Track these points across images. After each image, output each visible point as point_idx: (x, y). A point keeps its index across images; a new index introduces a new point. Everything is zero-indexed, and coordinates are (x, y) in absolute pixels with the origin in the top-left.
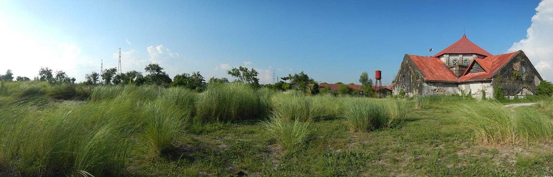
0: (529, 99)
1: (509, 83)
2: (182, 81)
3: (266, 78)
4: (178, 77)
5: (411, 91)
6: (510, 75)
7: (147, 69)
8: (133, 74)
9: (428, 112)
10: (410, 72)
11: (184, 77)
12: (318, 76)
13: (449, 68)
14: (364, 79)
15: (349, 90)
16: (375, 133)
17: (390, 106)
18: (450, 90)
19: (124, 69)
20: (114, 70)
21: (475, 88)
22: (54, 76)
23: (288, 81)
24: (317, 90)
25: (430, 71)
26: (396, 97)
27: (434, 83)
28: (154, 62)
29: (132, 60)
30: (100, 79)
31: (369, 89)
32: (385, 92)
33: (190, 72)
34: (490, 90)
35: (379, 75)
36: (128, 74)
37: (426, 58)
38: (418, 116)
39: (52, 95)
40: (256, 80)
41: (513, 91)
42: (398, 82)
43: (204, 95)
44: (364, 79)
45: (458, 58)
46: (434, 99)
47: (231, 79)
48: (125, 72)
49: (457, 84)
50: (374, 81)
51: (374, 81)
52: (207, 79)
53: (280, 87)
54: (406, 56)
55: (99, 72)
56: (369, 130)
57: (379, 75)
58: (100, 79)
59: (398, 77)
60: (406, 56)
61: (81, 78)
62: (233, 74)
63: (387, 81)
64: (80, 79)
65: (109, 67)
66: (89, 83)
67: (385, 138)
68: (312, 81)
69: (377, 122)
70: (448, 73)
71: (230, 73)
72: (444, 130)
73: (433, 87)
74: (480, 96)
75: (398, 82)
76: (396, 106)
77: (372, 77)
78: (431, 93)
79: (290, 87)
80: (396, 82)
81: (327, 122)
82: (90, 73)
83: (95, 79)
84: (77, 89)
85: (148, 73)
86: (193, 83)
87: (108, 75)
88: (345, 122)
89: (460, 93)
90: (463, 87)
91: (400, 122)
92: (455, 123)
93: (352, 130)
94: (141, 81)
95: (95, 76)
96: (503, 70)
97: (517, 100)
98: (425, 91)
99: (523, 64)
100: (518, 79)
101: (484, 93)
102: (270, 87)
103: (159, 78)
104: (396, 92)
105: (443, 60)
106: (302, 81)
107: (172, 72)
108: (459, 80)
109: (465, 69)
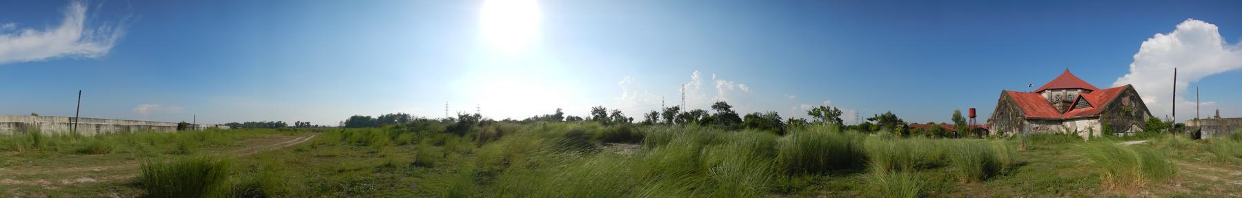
0: (1138, 136)
1: (1118, 119)
2: (755, 122)
3: (849, 119)
4: (748, 116)
5: (1010, 129)
6: (1119, 110)
7: (714, 107)
8: (699, 113)
9: (1036, 153)
10: (1008, 109)
11: (755, 116)
12: (908, 116)
13: (1052, 104)
14: (957, 118)
15: (941, 132)
16: (990, 183)
17: (999, 146)
18: (1054, 127)
19: (687, 108)
20: (677, 109)
21: (1081, 126)
22: (609, 115)
23: (874, 122)
24: (907, 131)
25: (1031, 107)
26: (993, 137)
27: (1036, 120)
28: (721, 100)
29: (697, 94)
30: (661, 119)
31: (960, 128)
32: (980, 131)
33: (763, 110)
34: (1097, 127)
35: (973, 113)
36: (693, 113)
37: (1025, 94)
38: (1024, 159)
39: (599, 138)
40: (840, 120)
41: (1122, 128)
42: (995, 121)
43: (787, 139)
44: (957, 118)
45: (1061, 93)
46: (1036, 138)
47: (810, 119)
48: (688, 110)
49: (1060, 121)
50: (968, 120)
51: (968, 120)
52: (785, 120)
53: (866, 128)
54: (1004, 92)
55: (660, 111)
56: (982, 179)
57: (973, 113)
58: (661, 119)
59: (995, 115)
60: (1004, 92)
61: (638, 116)
62: (815, 115)
63: (981, 120)
64: (639, 118)
65: (671, 105)
66: (648, 123)
67: (999, 185)
68: (901, 121)
69: (989, 169)
70: (1051, 109)
71: (810, 113)
72: (1063, 174)
73: (1035, 125)
74: (1086, 135)
75: (995, 121)
76: (1004, 147)
77: (966, 115)
78: (1033, 132)
79: (878, 128)
80: (993, 121)
81: (932, 172)
82: (649, 112)
83: (655, 119)
84: (632, 130)
85: (715, 111)
86: (771, 124)
87: (669, 114)
88: (949, 170)
89: (1064, 131)
90: (1068, 124)
91: (1015, 167)
92: (1070, 167)
93: (963, 181)
94: (707, 121)
95: (655, 114)
96: (1111, 105)
97: (1126, 138)
98: (1027, 130)
99: (1132, 98)
100: (1128, 114)
101: (1091, 131)
102: (854, 128)
103: (727, 118)
104: (992, 132)
105: (1045, 95)
106: (890, 121)
107: (742, 111)
108: (1063, 117)
109: (1069, 105)
